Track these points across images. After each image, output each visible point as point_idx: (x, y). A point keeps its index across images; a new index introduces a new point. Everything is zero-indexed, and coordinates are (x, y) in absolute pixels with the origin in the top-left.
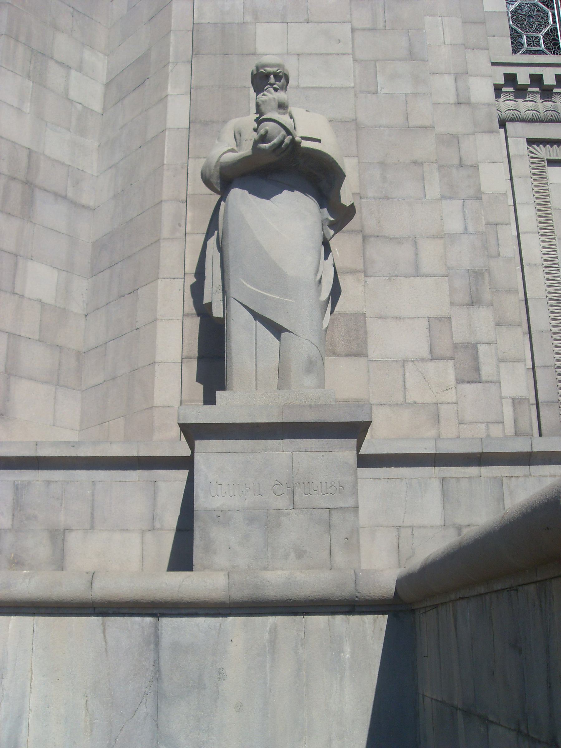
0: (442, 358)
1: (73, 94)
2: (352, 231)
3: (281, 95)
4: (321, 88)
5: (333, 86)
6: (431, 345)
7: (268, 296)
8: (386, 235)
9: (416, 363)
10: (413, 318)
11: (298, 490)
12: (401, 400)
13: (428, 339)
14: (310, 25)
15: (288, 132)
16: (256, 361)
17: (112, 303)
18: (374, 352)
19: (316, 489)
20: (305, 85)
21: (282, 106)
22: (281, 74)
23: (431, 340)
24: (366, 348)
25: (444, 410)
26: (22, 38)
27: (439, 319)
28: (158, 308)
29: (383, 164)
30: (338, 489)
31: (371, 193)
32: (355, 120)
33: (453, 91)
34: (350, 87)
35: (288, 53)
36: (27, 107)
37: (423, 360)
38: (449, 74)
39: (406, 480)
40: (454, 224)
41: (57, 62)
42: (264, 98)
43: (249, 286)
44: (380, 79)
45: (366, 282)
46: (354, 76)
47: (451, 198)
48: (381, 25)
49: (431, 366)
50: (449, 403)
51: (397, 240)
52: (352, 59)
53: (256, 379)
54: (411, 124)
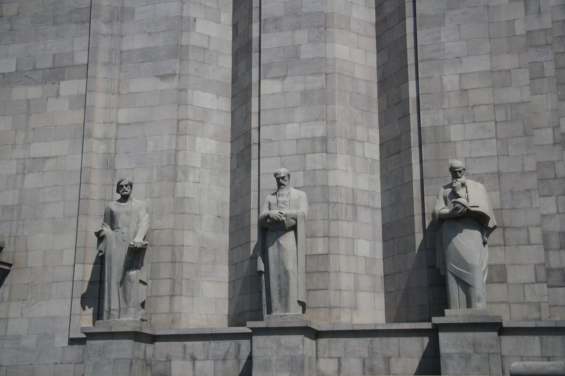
1: (367, 155)
12: (523, 301)
14: (475, 124)
15: (465, 207)
18: (510, 280)
25: (543, 305)
26: (344, 136)
27: (539, 265)
29: (512, 192)
33: (552, 137)
36: (349, 169)
37: (533, 283)
40: (552, 209)
44: (510, 148)
47: (550, 196)
48: (510, 118)
49: (536, 286)
54: (525, 170)
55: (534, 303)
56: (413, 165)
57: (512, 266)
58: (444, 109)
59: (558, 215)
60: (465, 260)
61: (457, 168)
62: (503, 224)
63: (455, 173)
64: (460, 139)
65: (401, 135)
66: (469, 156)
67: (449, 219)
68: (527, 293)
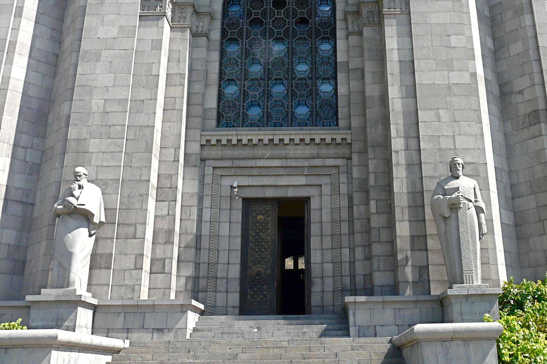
12: (122, 284)
26: (6, 141)
37: (132, 270)
41: (21, 147)
49: (134, 272)
55: (130, 286)
58: (89, 126)
59: (167, 217)
64: (96, 150)
66: (101, 165)
68: (126, 277)
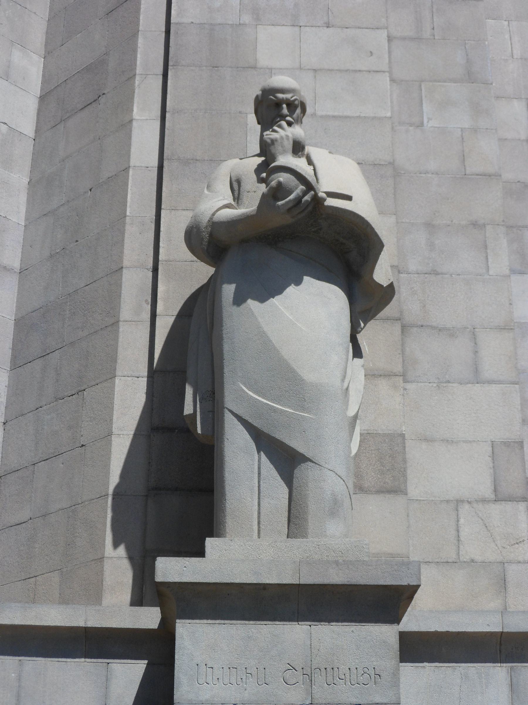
0: (511, 499)
2: (388, 319)
3: (298, 131)
4: (346, 117)
5: (362, 115)
6: (495, 481)
7: (278, 408)
8: (434, 324)
9: (475, 505)
10: (470, 442)
11: (319, 679)
12: (453, 557)
13: (492, 471)
14: (331, 30)
15: (309, 187)
16: (259, 498)
17: (45, 408)
18: (415, 489)
19: (343, 677)
20: (324, 113)
21: (298, 148)
22: (296, 102)
23: (495, 473)
24: (405, 482)
25: (512, 571)
27: (507, 444)
28: (115, 417)
30: (373, 677)
31: (412, 266)
32: (392, 164)
34: (386, 117)
35: (300, 68)
37: (484, 501)
38: (519, 98)
39: (461, 669)
42: (274, 135)
43: (251, 393)
44: (426, 107)
45: (405, 389)
46: (392, 102)
49: (495, 509)
50: (519, 562)
51: (450, 333)
52: (388, 79)
53: (259, 523)
54: (468, 172)
56: (135, 124)
57: (424, 445)
60: (293, 371)
61: (282, 91)
62: (401, 312)
63: (273, 108)
65: (106, 54)
67: (244, 241)
